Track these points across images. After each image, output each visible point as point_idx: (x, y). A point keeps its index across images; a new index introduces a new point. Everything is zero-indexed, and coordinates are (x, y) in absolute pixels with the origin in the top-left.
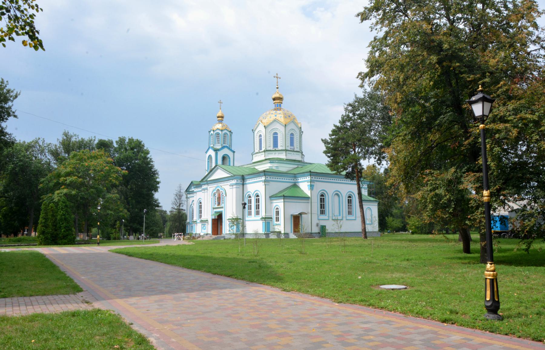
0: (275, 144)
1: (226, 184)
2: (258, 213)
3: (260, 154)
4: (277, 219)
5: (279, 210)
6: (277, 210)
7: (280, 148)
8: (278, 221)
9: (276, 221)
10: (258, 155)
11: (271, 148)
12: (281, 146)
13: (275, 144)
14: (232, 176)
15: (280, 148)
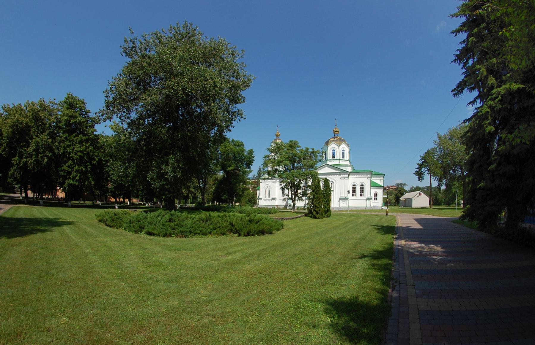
0: (343, 157)
1: (336, 176)
2: (362, 195)
3: (334, 161)
4: (376, 199)
5: (377, 194)
6: (376, 194)
7: (345, 159)
8: (377, 200)
9: (375, 200)
10: (332, 161)
11: (342, 158)
12: (346, 158)
13: (343, 157)
14: (344, 172)
15: (345, 159)
